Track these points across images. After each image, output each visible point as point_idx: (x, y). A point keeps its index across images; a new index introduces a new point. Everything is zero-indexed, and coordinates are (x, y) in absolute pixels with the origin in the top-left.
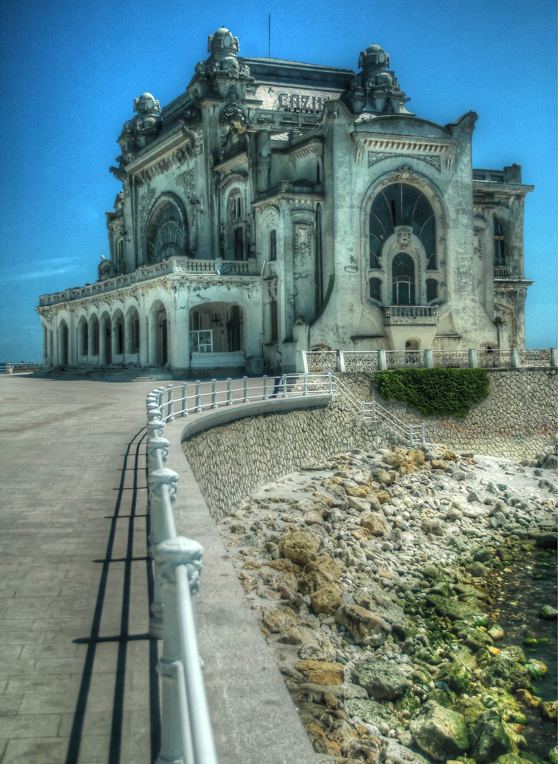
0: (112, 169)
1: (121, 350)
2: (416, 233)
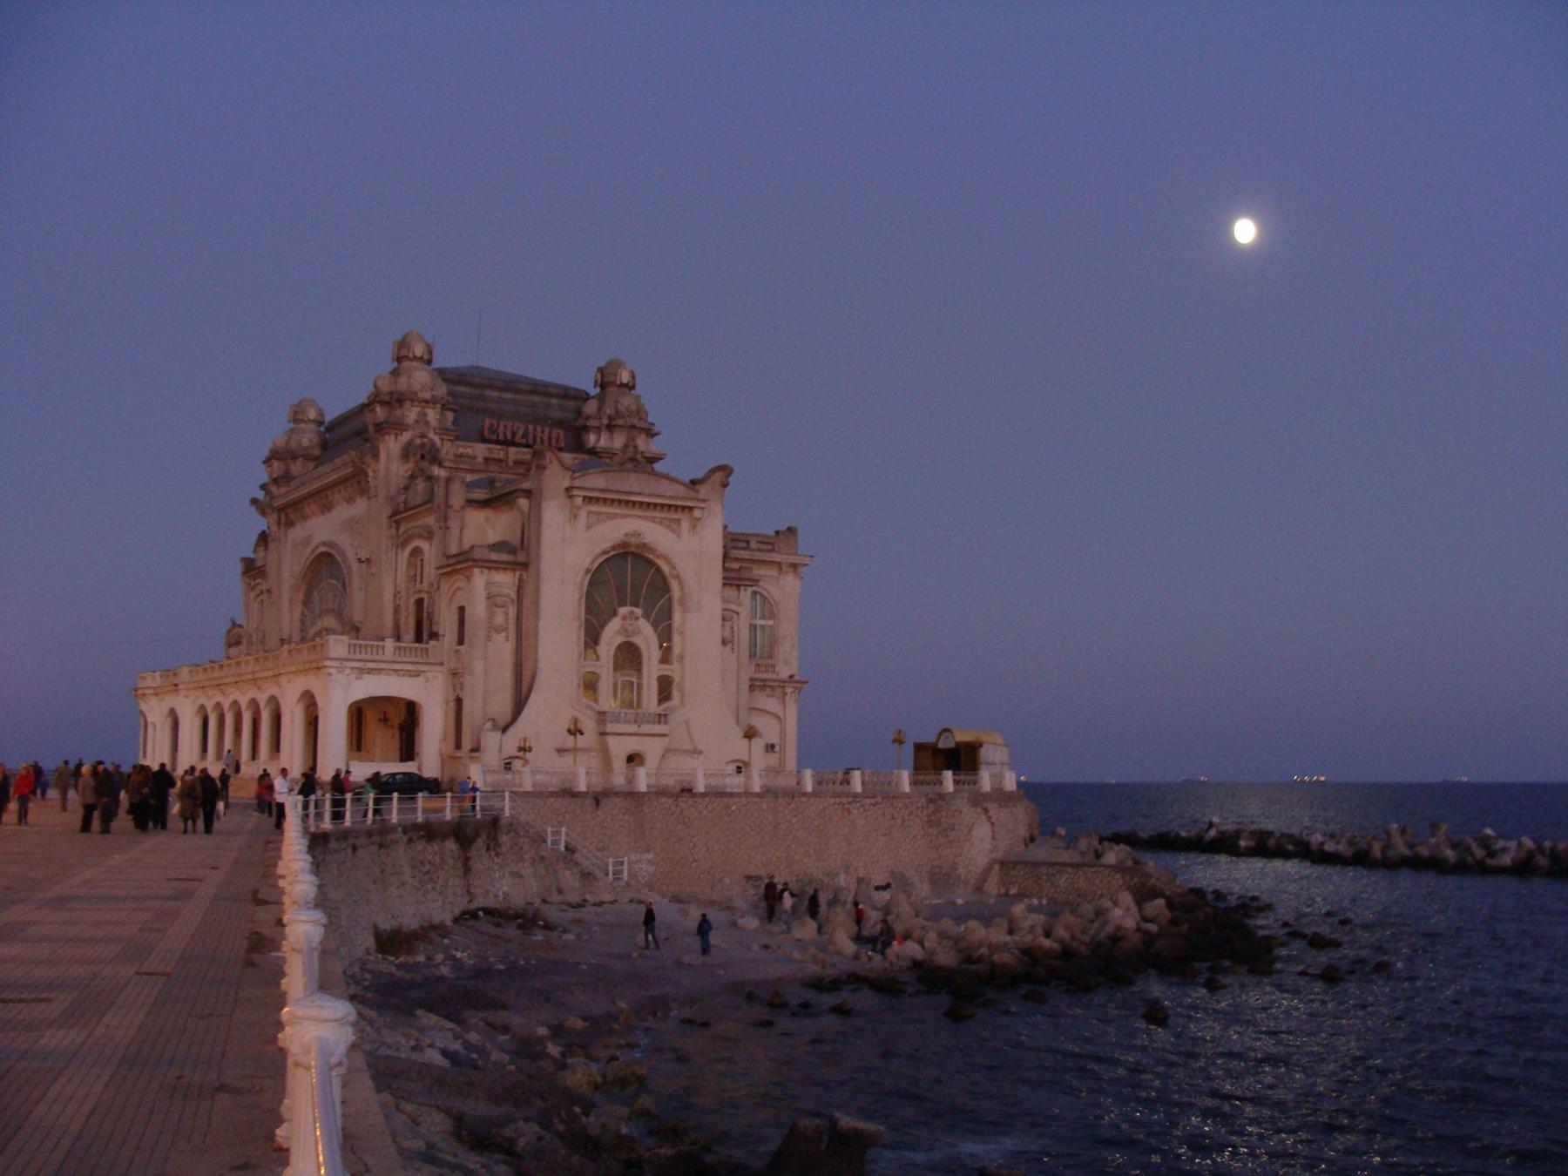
0: (254, 501)
2: (647, 616)
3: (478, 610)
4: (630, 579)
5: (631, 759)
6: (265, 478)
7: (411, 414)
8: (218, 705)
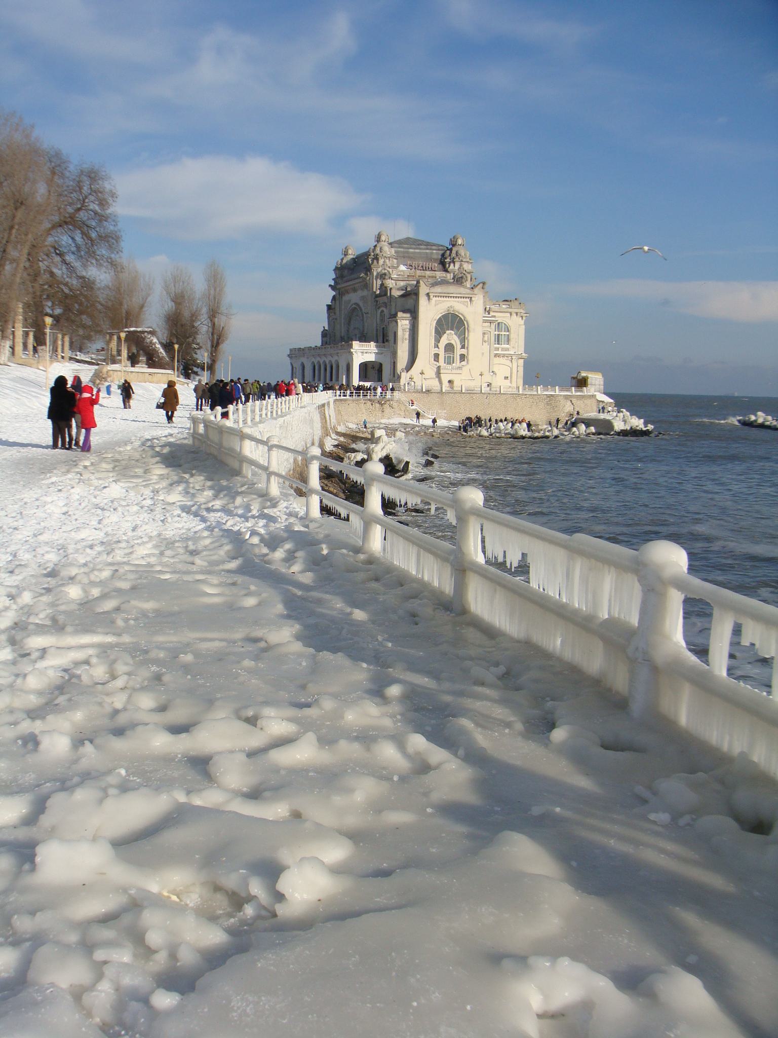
0: (330, 286)
1: (331, 380)
3: (400, 333)
4: (451, 322)
5: (450, 382)
6: (334, 276)
7: (381, 261)
8: (319, 362)
